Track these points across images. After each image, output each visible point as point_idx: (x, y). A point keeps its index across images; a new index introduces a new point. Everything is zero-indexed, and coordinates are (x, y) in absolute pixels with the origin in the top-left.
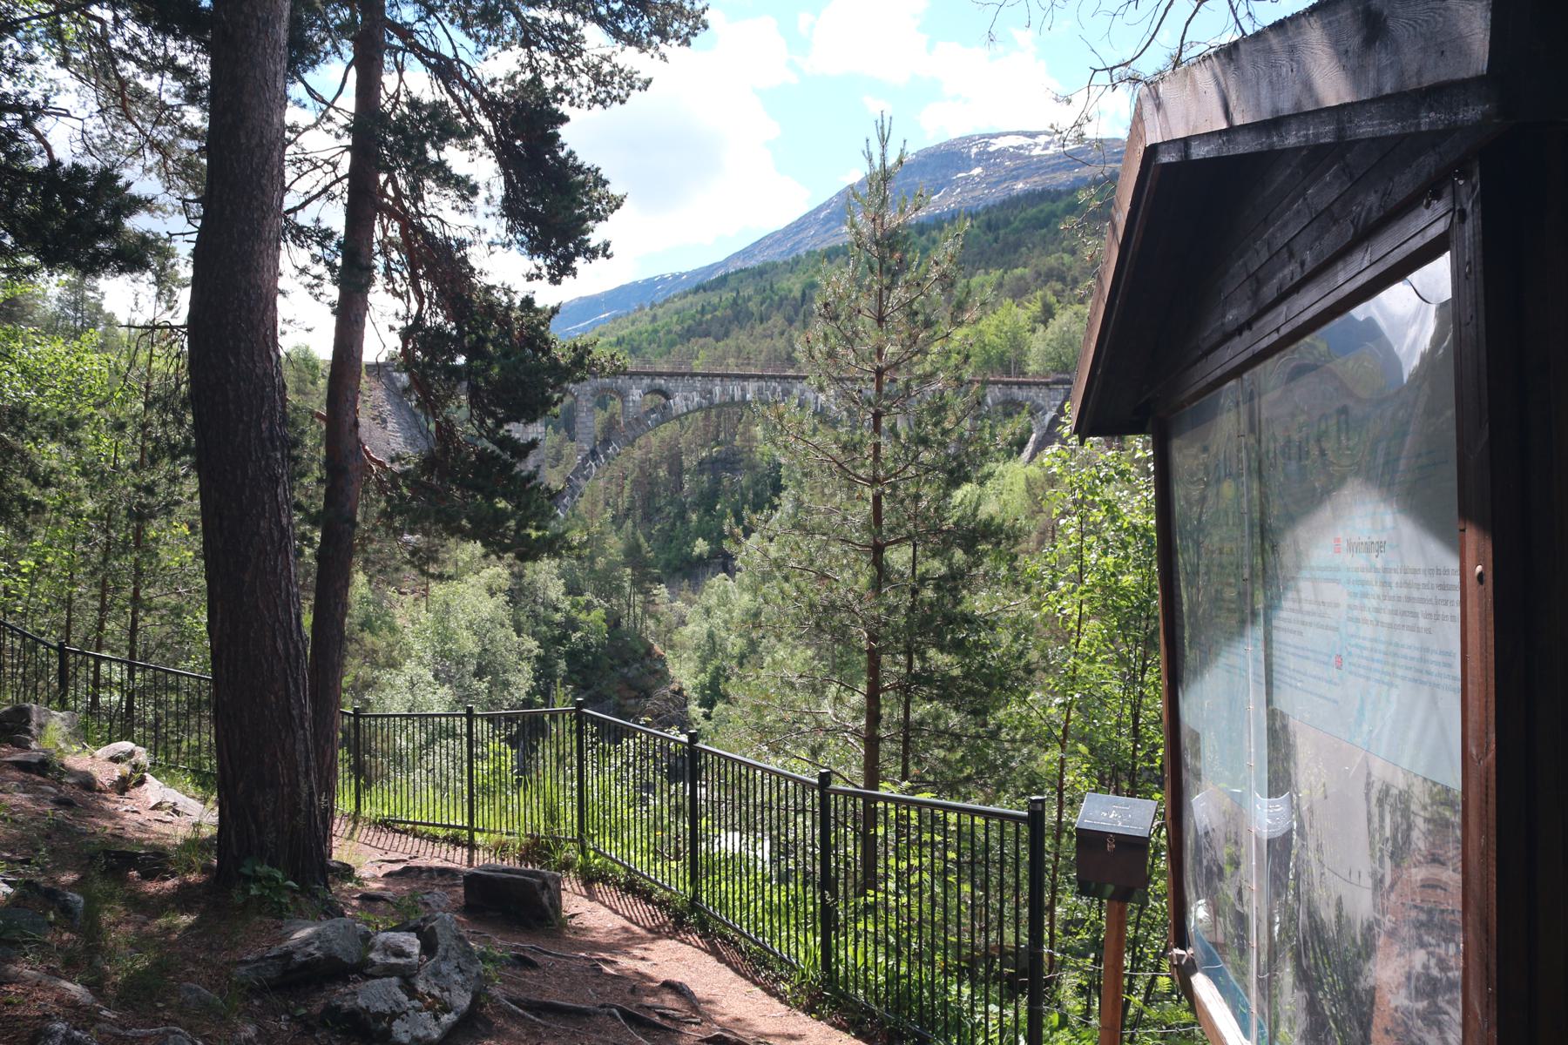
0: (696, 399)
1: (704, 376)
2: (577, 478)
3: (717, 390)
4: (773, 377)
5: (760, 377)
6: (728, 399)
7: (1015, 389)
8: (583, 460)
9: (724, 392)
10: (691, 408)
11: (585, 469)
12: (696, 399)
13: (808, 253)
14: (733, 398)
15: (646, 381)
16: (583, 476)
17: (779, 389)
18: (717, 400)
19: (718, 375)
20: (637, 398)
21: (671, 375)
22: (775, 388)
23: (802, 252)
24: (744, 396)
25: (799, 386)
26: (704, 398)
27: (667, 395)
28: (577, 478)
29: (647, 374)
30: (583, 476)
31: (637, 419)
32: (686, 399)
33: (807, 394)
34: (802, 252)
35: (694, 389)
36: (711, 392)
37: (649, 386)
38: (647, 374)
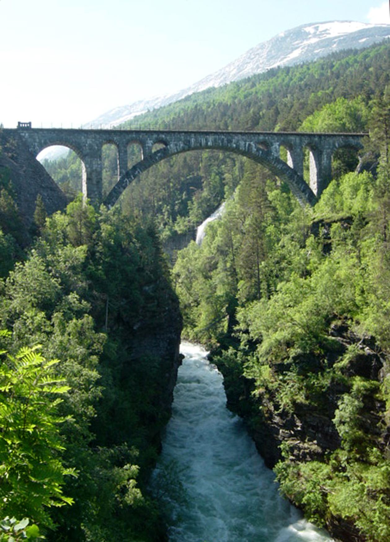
0: (182, 145)
1: (185, 132)
3: (193, 140)
7: (351, 139)
9: (196, 142)
10: (179, 150)
11: (123, 183)
13: (231, 83)
14: (201, 144)
15: (155, 136)
17: (226, 139)
22: (223, 139)
23: (228, 83)
24: (207, 143)
25: (236, 137)
26: (186, 144)
30: (122, 187)
32: (176, 145)
33: (241, 142)
34: (228, 83)
35: (180, 140)
36: (189, 141)
37: (156, 139)
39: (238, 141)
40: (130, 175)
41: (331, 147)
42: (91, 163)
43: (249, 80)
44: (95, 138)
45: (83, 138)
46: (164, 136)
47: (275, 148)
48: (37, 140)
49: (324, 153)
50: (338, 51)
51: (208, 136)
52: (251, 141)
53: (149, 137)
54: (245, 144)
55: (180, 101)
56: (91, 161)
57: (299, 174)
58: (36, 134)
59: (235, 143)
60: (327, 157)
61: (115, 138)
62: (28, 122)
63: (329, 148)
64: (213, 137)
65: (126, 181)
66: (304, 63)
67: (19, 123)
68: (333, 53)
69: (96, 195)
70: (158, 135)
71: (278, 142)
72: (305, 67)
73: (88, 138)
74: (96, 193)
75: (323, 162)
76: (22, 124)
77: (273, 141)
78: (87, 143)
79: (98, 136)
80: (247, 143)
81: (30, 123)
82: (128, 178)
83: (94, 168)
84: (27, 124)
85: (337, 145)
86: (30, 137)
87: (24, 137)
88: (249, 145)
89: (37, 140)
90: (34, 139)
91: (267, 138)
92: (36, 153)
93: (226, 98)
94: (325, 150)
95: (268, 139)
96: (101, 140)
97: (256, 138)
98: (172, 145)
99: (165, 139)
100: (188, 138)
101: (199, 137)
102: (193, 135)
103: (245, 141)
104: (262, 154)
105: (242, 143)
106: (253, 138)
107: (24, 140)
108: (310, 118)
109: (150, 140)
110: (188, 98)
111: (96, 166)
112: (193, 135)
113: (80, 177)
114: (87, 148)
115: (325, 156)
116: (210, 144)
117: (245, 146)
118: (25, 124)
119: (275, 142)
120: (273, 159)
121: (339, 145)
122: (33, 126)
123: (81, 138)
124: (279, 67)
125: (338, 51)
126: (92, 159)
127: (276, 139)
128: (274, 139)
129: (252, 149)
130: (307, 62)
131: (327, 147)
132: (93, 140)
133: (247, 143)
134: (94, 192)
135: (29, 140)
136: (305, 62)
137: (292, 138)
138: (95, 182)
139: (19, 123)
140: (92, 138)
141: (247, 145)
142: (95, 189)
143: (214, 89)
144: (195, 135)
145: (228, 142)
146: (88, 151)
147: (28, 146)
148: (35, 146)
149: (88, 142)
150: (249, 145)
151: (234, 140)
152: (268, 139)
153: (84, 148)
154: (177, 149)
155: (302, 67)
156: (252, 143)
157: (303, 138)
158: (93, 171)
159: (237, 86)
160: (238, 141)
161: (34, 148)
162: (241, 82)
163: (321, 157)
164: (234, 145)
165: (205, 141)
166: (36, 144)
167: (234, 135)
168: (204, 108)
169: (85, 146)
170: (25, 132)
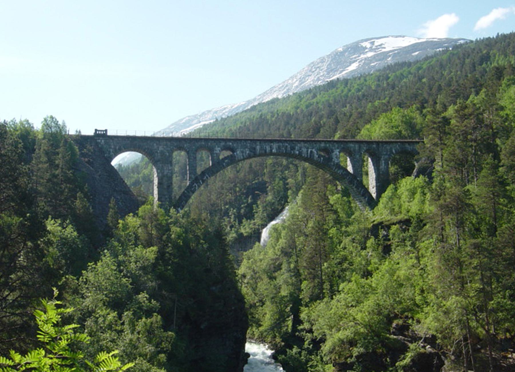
0: (247, 152)
1: (251, 140)
3: (258, 147)
7: (407, 145)
9: (261, 149)
11: (192, 187)
12: (247, 152)
13: (294, 94)
14: (266, 151)
15: (223, 144)
17: (289, 146)
22: (287, 146)
23: (291, 94)
24: (271, 150)
25: (299, 145)
30: (191, 191)
32: (242, 152)
33: (303, 149)
34: (291, 94)
35: (247, 147)
36: (255, 149)
37: (224, 146)
39: (301, 148)
41: (389, 153)
43: (310, 91)
44: (166, 145)
45: (155, 144)
46: (231, 144)
47: (336, 154)
49: (382, 159)
50: (393, 64)
51: (272, 144)
52: (313, 148)
54: (307, 151)
55: (246, 111)
56: (162, 166)
57: (358, 179)
59: (298, 150)
60: (385, 163)
61: (185, 146)
62: (104, 129)
63: (386, 154)
64: (277, 144)
65: (195, 186)
66: (361, 75)
67: (96, 130)
68: (388, 66)
70: (226, 143)
71: (338, 148)
72: (362, 79)
73: (160, 145)
75: (381, 167)
76: (99, 131)
79: (169, 144)
80: (309, 150)
81: (106, 131)
82: (197, 183)
83: (165, 173)
84: (103, 131)
85: (394, 151)
87: (100, 143)
88: (311, 152)
89: (113, 147)
91: (328, 145)
92: (111, 159)
93: (289, 108)
94: (383, 157)
96: (171, 147)
97: (318, 145)
98: (238, 152)
101: (264, 144)
102: (258, 143)
103: (308, 148)
104: (323, 160)
105: (304, 150)
106: (315, 145)
107: (100, 146)
108: (368, 126)
109: (218, 147)
110: (254, 108)
111: (167, 171)
113: (152, 182)
114: (159, 154)
115: (383, 162)
117: (307, 153)
118: (101, 131)
120: (334, 165)
122: (109, 133)
124: (338, 79)
125: (393, 64)
127: (336, 146)
129: (313, 156)
130: (365, 74)
131: (385, 153)
132: (165, 147)
133: (309, 150)
134: (165, 195)
135: (105, 146)
136: (362, 74)
137: (352, 145)
138: (165, 187)
139: (96, 130)
143: (277, 99)
144: (260, 143)
145: (291, 150)
148: (110, 151)
151: (297, 147)
155: (359, 79)
156: (314, 150)
157: (362, 145)
159: (299, 96)
160: (301, 148)
161: (109, 153)
163: (379, 163)
164: (297, 152)
165: (269, 149)
166: (111, 150)
167: (297, 143)
168: (269, 117)
169: (157, 152)
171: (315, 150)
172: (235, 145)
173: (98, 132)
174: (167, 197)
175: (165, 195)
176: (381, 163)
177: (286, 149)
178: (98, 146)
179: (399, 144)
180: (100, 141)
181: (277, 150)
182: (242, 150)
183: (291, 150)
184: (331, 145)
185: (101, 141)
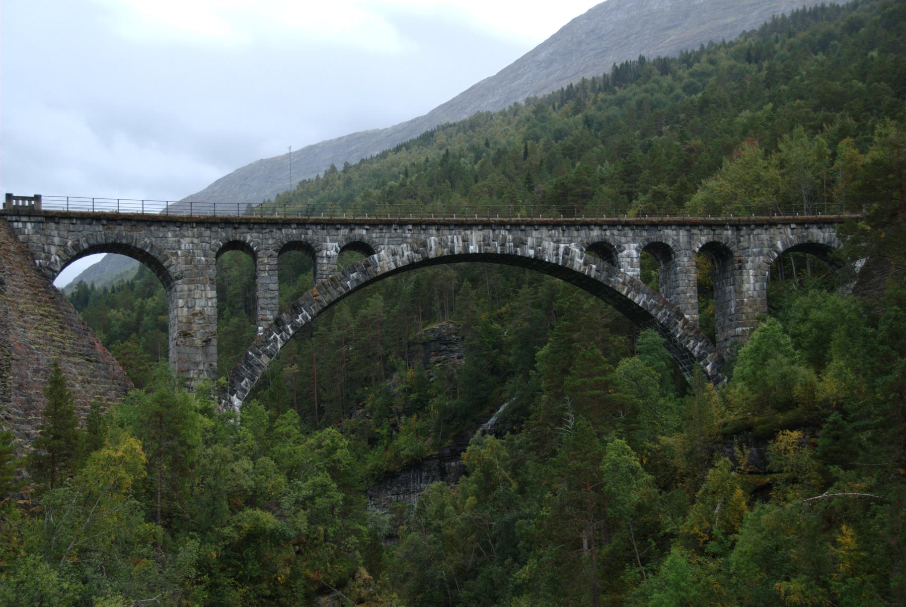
1: (416, 224)
2: (259, 355)
3: (433, 241)
4: (501, 225)
5: (486, 225)
6: (446, 251)
8: (265, 330)
9: (441, 244)
10: (400, 264)
11: (268, 343)
12: (406, 253)
14: (452, 251)
15: (344, 232)
16: (265, 352)
17: (510, 237)
18: (432, 255)
19: (433, 224)
20: (333, 253)
21: (374, 225)
22: (505, 238)
24: (466, 248)
25: (535, 234)
26: (417, 252)
27: (367, 249)
28: (259, 355)
29: (346, 224)
30: (265, 352)
31: (332, 279)
32: (394, 254)
33: (546, 244)
35: (404, 240)
36: (424, 245)
38: (346, 224)
40: (284, 324)
41: (766, 250)
42: (189, 295)
44: (200, 236)
45: (170, 235)
46: (364, 232)
47: (628, 256)
48: (57, 240)
49: (749, 265)
50: (788, 15)
51: (468, 232)
52: (570, 242)
53: (329, 234)
54: (558, 248)
55: (407, 146)
56: (190, 290)
57: (687, 316)
58: (53, 225)
59: (532, 248)
61: (249, 238)
62: (32, 195)
63: (760, 253)
64: (481, 233)
65: (275, 339)
67: (9, 197)
69: (201, 372)
70: (352, 230)
71: (634, 241)
72: (704, 58)
73: (184, 236)
74: (201, 367)
75: (746, 286)
76: (17, 198)
77: (623, 239)
78: (180, 249)
79: (208, 233)
80: (562, 246)
81: (37, 198)
82: (280, 332)
83: (197, 309)
84: (30, 199)
85: (779, 245)
86: (37, 232)
88: (567, 251)
89: (57, 240)
90: (48, 236)
91: (608, 233)
92: (55, 274)
95: (613, 234)
96: (213, 242)
97: (583, 233)
99: (366, 238)
100: (423, 237)
101: (446, 232)
102: (433, 231)
103: (558, 241)
104: (597, 271)
105: (549, 245)
106: (575, 233)
107: (21, 237)
109: (332, 241)
110: (427, 138)
111: (202, 302)
112: (433, 231)
115: (751, 272)
116: (473, 249)
117: (557, 255)
118: (24, 199)
119: (627, 242)
120: (624, 284)
121: (783, 244)
122: (47, 205)
123: (165, 237)
126: (193, 287)
127: (631, 234)
128: (625, 236)
129: (572, 260)
132: (196, 241)
133: (562, 246)
134: (197, 364)
135: (35, 238)
136: (706, 45)
137: (669, 232)
138: (198, 342)
139: (9, 197)
140: (193, 236)
141: (561, 251)
142: (199, 358)
143: (489, 116)
144: (438, 230)
145: (516, 246)
146: (183, 267)
147: (32, 254)
148: (49, 253)
149: (183, 247)
150: (567, 251)
152: (613, 234)
153: (173, 259)
154: (395, 262)
158: (195, 315)
159: (540, 108)
161: (48, 258)
162: (550, 100)
163: (741, 274)
166: (53, 249)
168: (466, 163)
169: (176, 254)
170: (24, 219)
171: (577, 246)
172: (374, 235)
173: (14, 202)
174: (201, 367)
175: (197, 364)
176: (745, 277)
177: (503, 245)
178: (16, 238)
179: (793, 226)
180: (20, 225)
181: (480, 247)
182: (392, 247)
183: (516, 246)
184: (616, 232)
185: (25, 227)
